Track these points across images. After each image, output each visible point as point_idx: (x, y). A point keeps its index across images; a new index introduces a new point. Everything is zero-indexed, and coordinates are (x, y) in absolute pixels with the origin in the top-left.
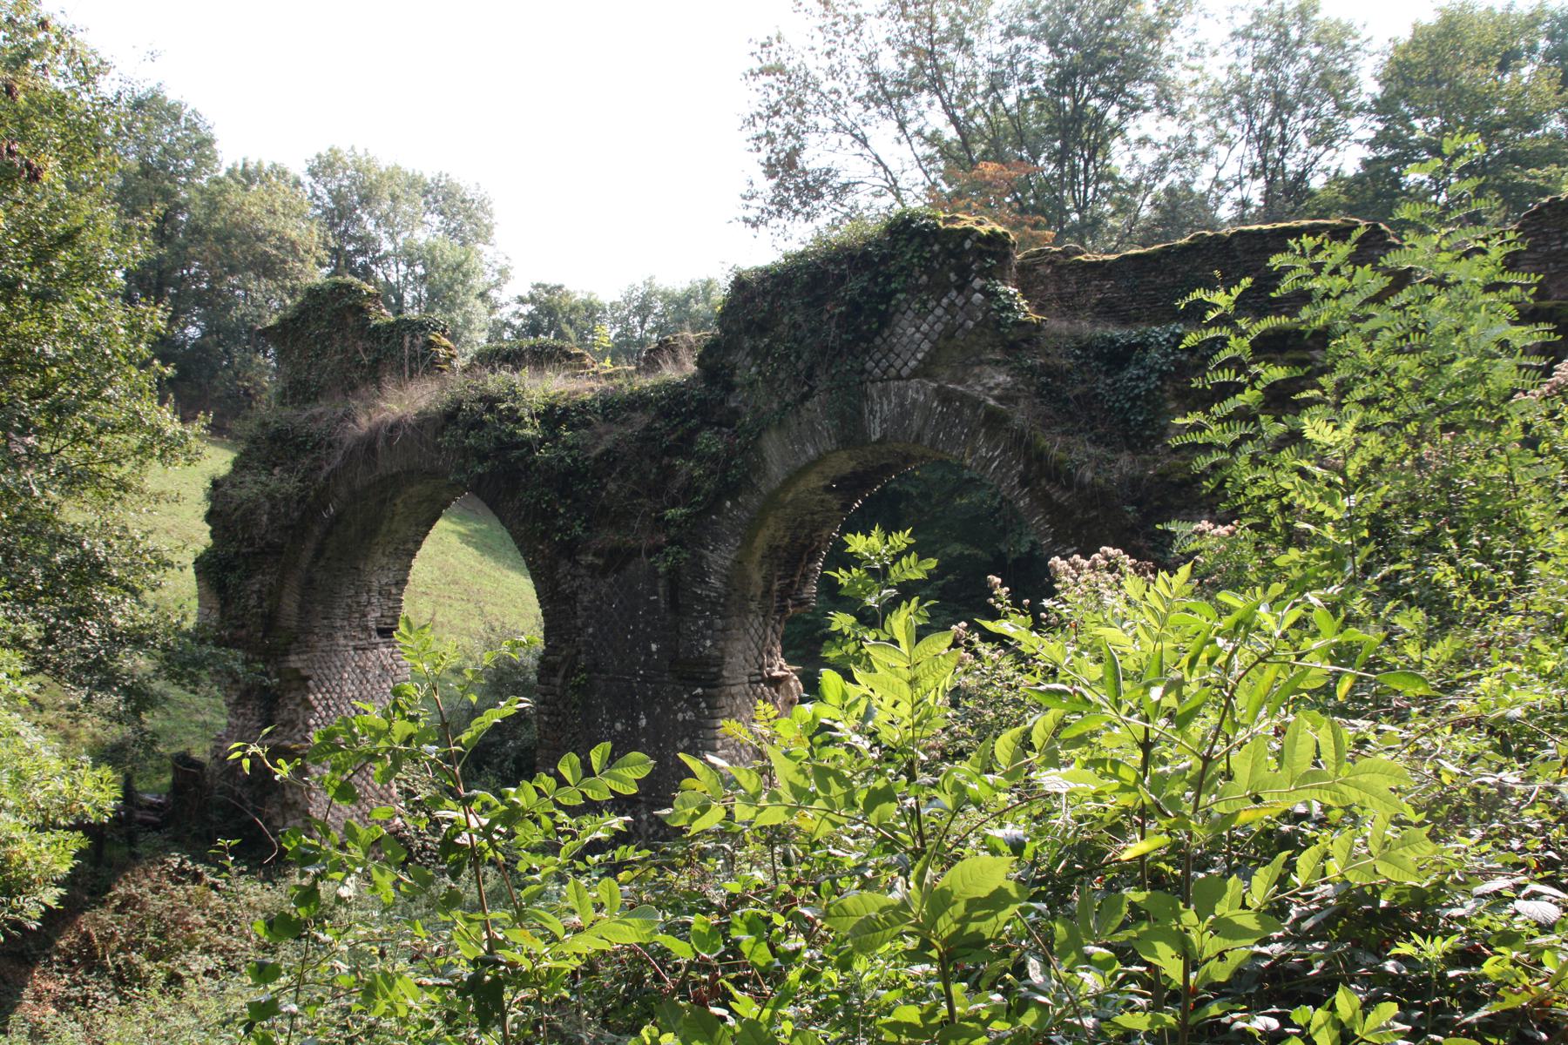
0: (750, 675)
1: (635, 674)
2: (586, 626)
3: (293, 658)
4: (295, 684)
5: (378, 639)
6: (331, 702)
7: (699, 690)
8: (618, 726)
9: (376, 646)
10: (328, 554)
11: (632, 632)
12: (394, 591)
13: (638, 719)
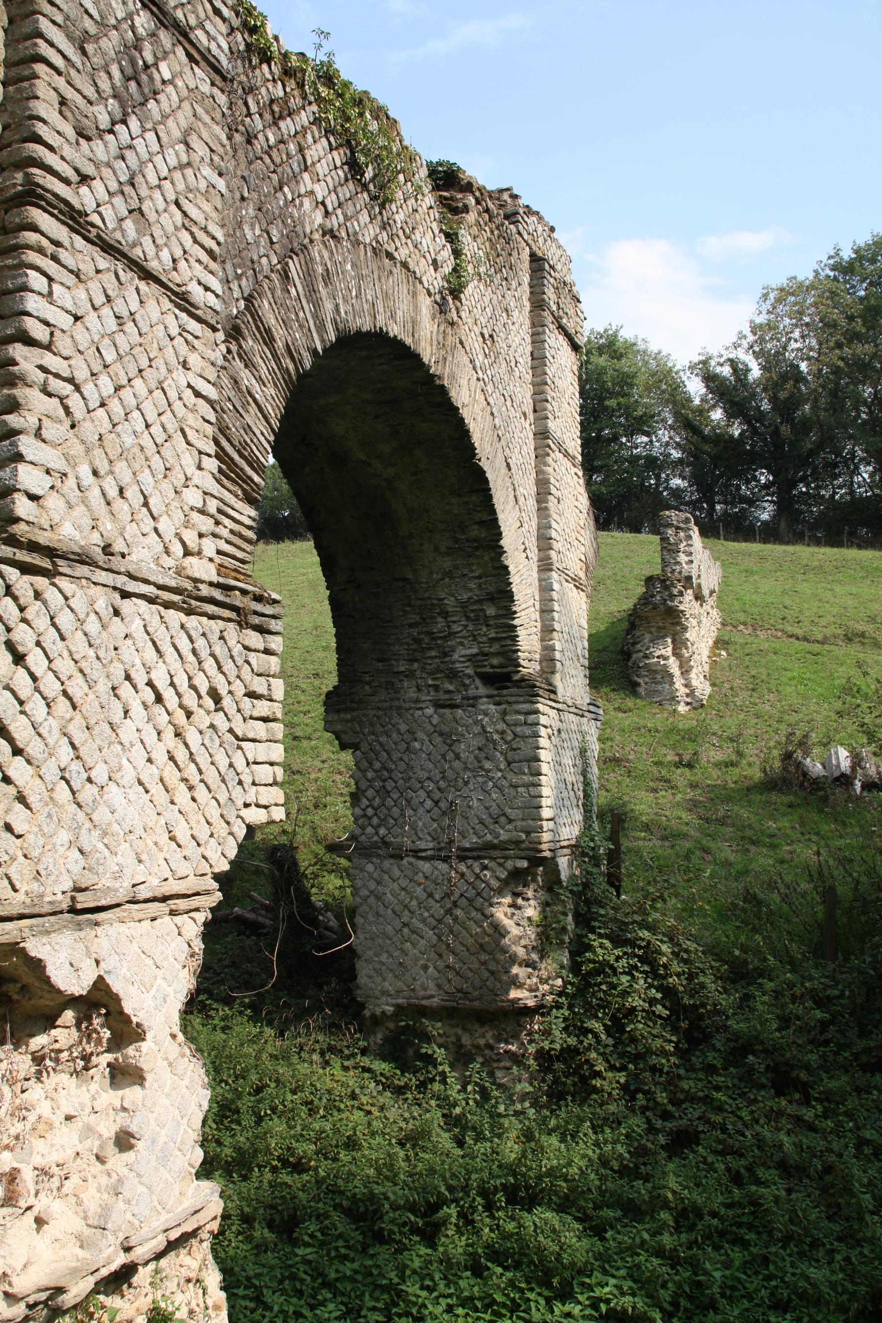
5: (482, 690)
6: (390, 785)
12: (491, 611)
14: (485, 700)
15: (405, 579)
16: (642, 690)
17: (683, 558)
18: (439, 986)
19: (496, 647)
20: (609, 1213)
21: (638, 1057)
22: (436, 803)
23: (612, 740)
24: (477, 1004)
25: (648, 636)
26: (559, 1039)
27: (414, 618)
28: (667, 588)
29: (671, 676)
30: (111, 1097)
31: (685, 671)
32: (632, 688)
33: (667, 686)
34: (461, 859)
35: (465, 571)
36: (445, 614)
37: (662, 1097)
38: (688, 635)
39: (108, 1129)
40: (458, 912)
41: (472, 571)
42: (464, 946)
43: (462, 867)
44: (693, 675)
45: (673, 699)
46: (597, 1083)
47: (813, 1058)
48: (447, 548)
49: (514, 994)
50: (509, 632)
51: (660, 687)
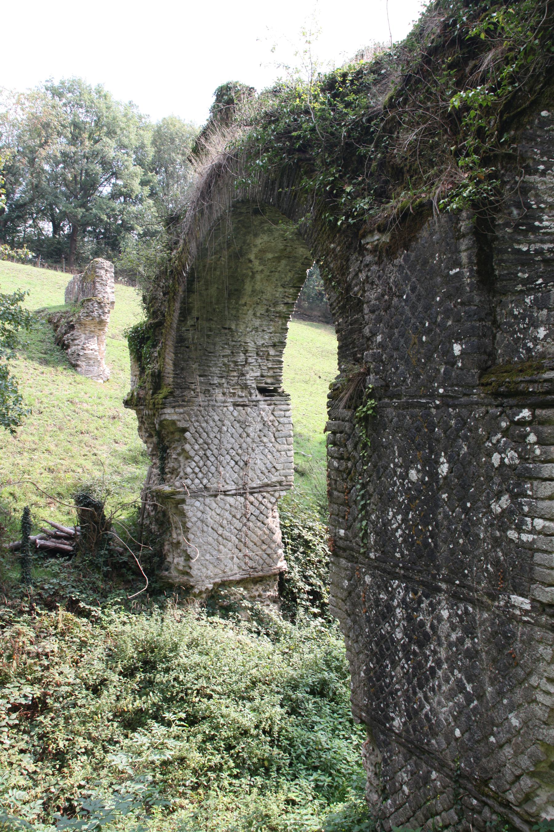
1: (433, 396)
2: (374, 335)
3: (168, 410)
4: (177, 436)
5: (260, 397)
6: (209, 453)
7: (526, 413)
8: (413, 475)
10: (195, 314)
11: (428, 332)
12: (272, 352)
13: (437, 463)
14: (262, 402)
15: (230, 329)
18: (239, 567)
19: (271, 373)
22: (236, 463)
24: (261, 574)
25: (83, 336)
27: (228, 352)
28: (101, 307)
33: (96, 368)
34: (251, 493)
35: (266, 329)
40: (251, 524)
41: (269, 329)
42: (253, 542)
43: (251, 498)
48: (261, 314)
51: (91, 368)
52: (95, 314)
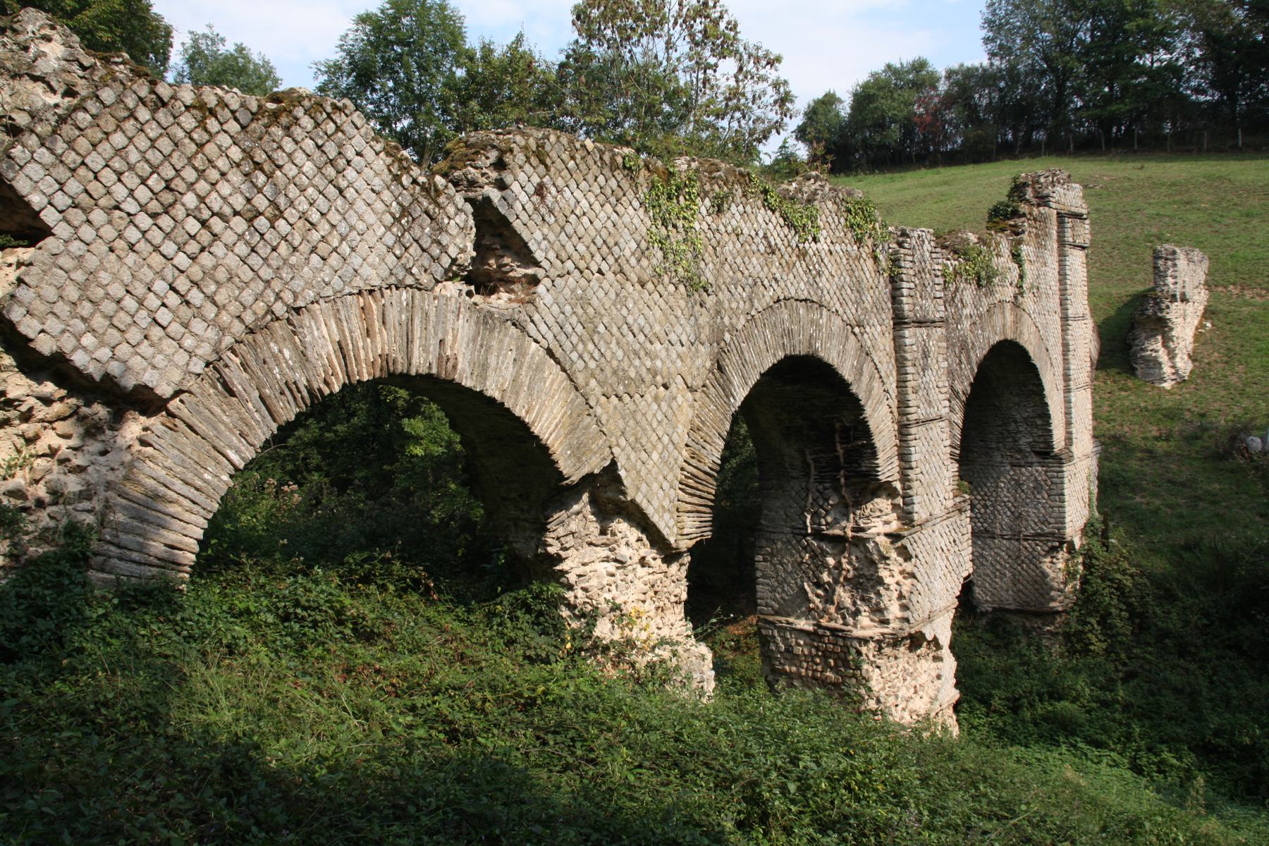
0: (793, 527)
5: (1035, 459)
9: (1031, 464)
16: (1139, 372)
17: (1170, 280)
20: (1094, 705)
21: (1112, 636)
23: (1114, 420)
25: (1144, 335)
26: (1075, 626)
28: (1157, 304)
29: (1160, 364)
30: (934, 665)
31: (1172, 355)
32: (1131, 371)
34: (1026, 540)
36: (1016, 422)
37: (1123, 656)
38: (1173, 333)
39: (934, 674)
44: (1178, 360)
45: (1163, 380)
46: (1092, 647)
47: (1199, 642)
49: (1052, 604)
50: (1048, 433)
52: (1150, 312)
